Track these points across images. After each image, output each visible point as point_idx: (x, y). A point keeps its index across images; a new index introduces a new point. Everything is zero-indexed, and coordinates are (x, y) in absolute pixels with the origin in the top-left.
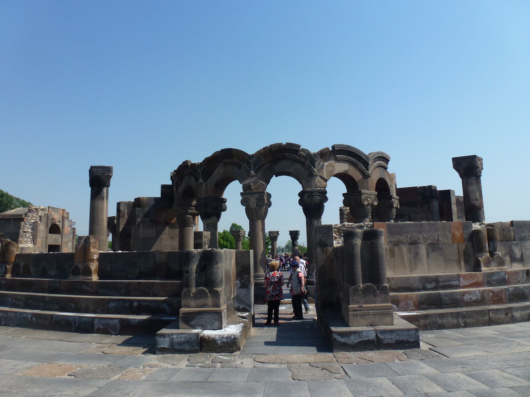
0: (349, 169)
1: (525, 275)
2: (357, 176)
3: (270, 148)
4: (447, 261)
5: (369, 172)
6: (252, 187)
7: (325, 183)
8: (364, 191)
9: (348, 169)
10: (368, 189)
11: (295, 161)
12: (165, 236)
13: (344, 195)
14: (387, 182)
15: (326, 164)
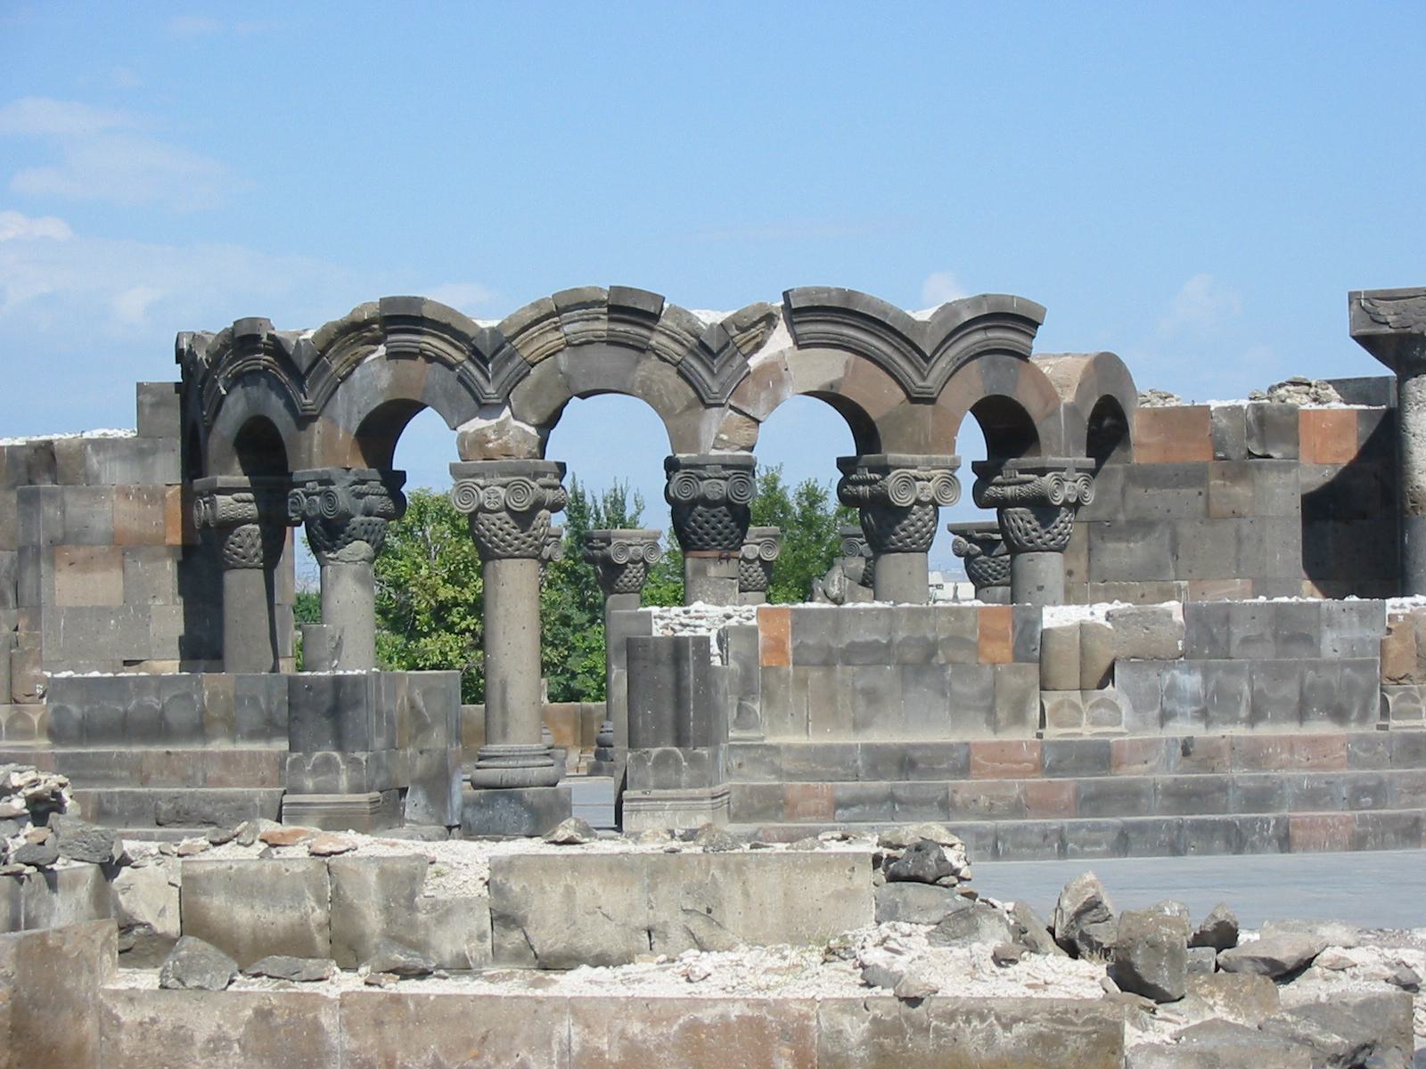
0: (846, 374)
1: (1179, 751)
2: (880, 397)
3: (557, 307)
4: (959, 709)
5: (928, 383)
6: (491, 445)
7: (751, 431)
8: (903, 456)
9: (841, 375)
10: (917, 449)
11: (642, 349)
12: (159, 602)
13: (843, 463)
14: (1024, 409)
15: (754, 362)
